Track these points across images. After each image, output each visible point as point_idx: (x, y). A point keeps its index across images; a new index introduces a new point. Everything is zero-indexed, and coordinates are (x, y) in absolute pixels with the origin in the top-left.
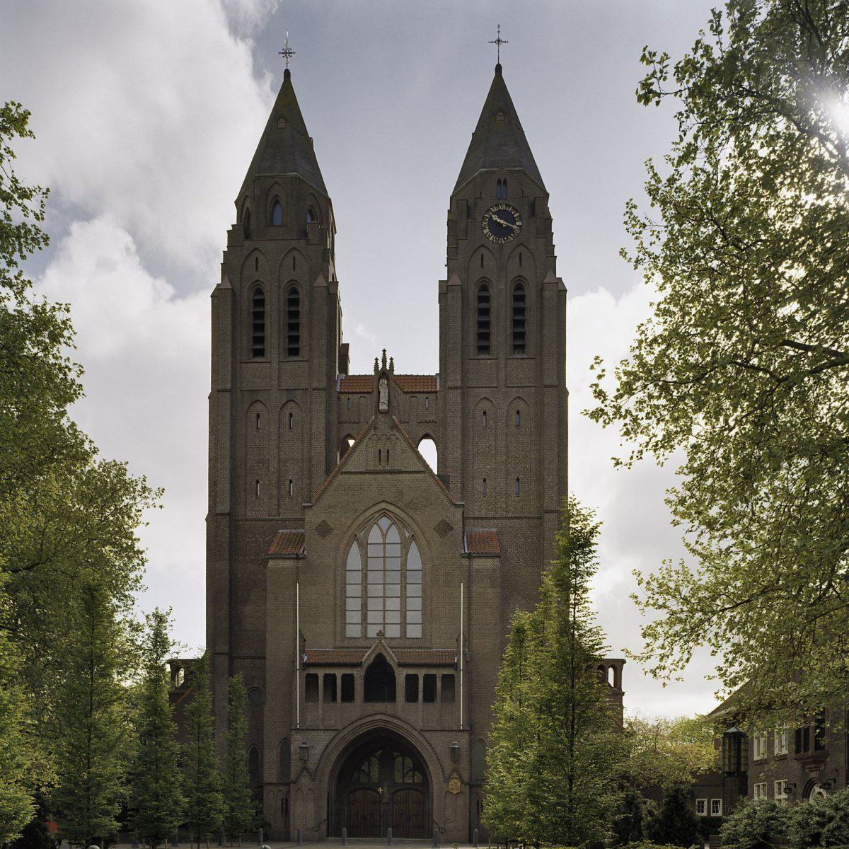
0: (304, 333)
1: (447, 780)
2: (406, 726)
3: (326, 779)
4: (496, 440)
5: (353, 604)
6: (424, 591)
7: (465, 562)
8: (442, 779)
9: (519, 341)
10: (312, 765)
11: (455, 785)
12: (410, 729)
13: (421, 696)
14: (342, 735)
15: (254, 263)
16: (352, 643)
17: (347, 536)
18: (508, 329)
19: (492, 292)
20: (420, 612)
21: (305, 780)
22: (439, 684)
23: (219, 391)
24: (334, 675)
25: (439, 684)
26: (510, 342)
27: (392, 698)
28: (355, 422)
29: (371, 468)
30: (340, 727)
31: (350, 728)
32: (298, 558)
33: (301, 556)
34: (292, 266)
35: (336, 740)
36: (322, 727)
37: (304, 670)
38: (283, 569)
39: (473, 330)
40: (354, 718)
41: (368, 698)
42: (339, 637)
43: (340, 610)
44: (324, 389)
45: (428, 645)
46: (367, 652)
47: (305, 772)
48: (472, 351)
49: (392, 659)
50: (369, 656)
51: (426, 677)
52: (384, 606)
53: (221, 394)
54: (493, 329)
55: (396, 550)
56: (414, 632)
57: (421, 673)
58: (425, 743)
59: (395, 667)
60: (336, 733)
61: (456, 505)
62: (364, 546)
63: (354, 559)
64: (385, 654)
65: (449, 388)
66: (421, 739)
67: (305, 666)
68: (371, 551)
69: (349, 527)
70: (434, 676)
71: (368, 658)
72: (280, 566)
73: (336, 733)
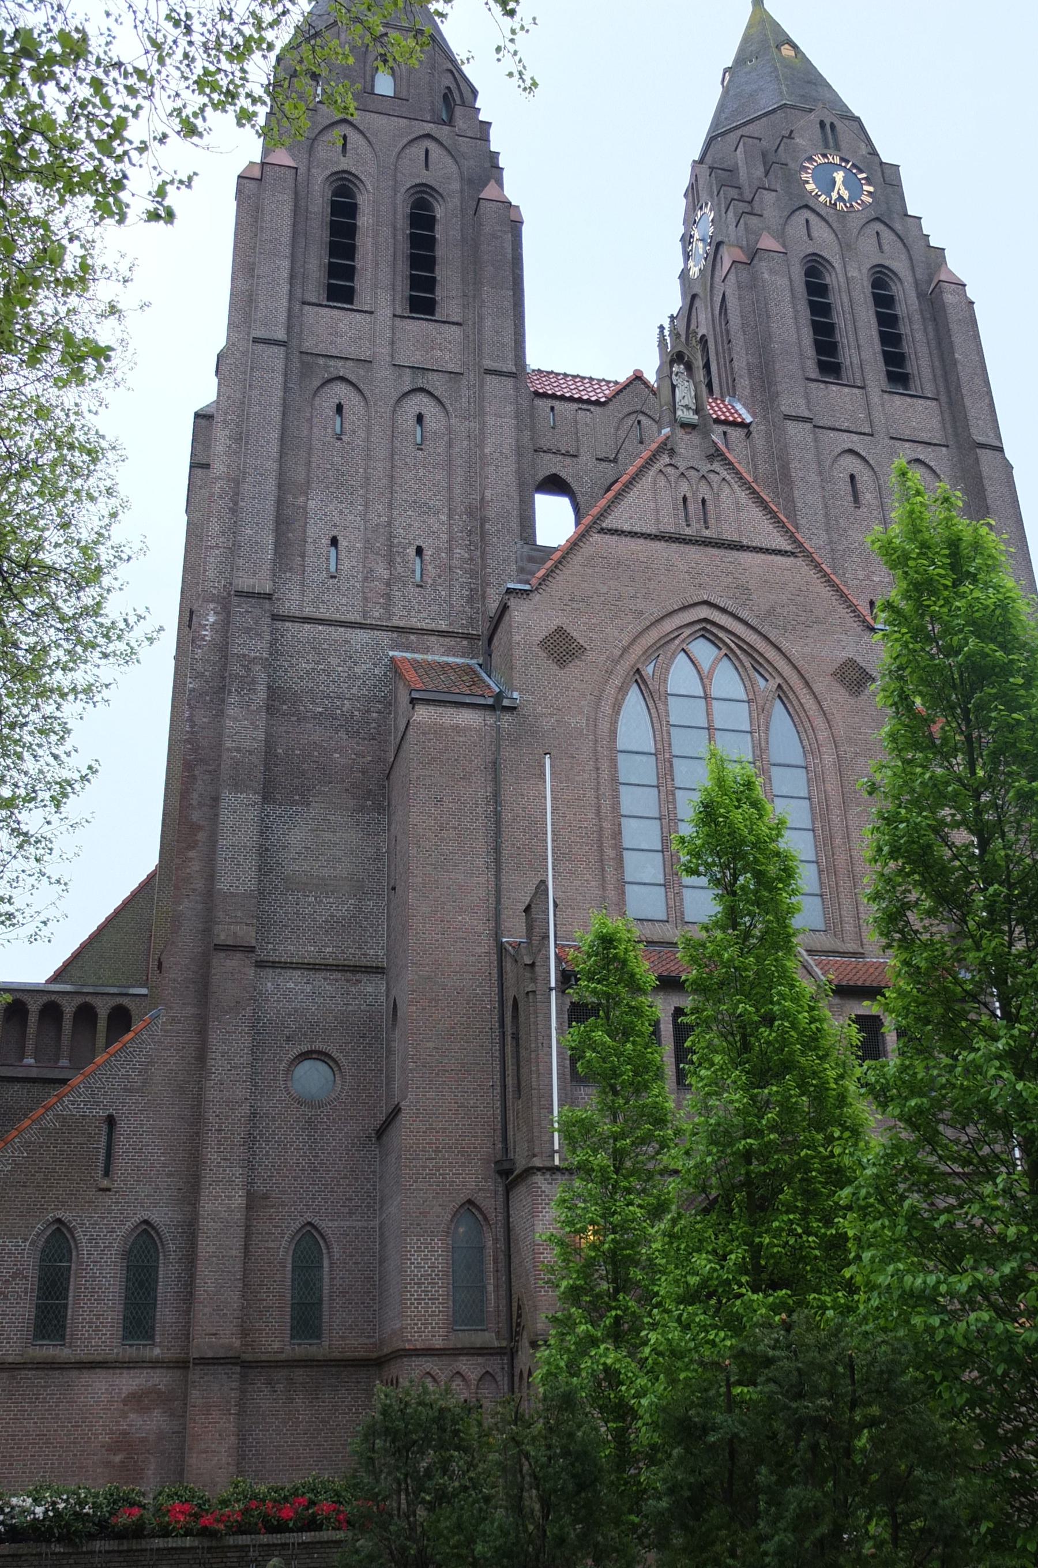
15: (340, 143)
29: (669, 525)
32: (497, 706)
38: (456, 728)
45: (851, 947)
53: (261, 347)
55: (738, 716)
62: (655, 697)
63: (634, 725)
65: (788, 417)
68: (677, 712)
69: (625, 650)
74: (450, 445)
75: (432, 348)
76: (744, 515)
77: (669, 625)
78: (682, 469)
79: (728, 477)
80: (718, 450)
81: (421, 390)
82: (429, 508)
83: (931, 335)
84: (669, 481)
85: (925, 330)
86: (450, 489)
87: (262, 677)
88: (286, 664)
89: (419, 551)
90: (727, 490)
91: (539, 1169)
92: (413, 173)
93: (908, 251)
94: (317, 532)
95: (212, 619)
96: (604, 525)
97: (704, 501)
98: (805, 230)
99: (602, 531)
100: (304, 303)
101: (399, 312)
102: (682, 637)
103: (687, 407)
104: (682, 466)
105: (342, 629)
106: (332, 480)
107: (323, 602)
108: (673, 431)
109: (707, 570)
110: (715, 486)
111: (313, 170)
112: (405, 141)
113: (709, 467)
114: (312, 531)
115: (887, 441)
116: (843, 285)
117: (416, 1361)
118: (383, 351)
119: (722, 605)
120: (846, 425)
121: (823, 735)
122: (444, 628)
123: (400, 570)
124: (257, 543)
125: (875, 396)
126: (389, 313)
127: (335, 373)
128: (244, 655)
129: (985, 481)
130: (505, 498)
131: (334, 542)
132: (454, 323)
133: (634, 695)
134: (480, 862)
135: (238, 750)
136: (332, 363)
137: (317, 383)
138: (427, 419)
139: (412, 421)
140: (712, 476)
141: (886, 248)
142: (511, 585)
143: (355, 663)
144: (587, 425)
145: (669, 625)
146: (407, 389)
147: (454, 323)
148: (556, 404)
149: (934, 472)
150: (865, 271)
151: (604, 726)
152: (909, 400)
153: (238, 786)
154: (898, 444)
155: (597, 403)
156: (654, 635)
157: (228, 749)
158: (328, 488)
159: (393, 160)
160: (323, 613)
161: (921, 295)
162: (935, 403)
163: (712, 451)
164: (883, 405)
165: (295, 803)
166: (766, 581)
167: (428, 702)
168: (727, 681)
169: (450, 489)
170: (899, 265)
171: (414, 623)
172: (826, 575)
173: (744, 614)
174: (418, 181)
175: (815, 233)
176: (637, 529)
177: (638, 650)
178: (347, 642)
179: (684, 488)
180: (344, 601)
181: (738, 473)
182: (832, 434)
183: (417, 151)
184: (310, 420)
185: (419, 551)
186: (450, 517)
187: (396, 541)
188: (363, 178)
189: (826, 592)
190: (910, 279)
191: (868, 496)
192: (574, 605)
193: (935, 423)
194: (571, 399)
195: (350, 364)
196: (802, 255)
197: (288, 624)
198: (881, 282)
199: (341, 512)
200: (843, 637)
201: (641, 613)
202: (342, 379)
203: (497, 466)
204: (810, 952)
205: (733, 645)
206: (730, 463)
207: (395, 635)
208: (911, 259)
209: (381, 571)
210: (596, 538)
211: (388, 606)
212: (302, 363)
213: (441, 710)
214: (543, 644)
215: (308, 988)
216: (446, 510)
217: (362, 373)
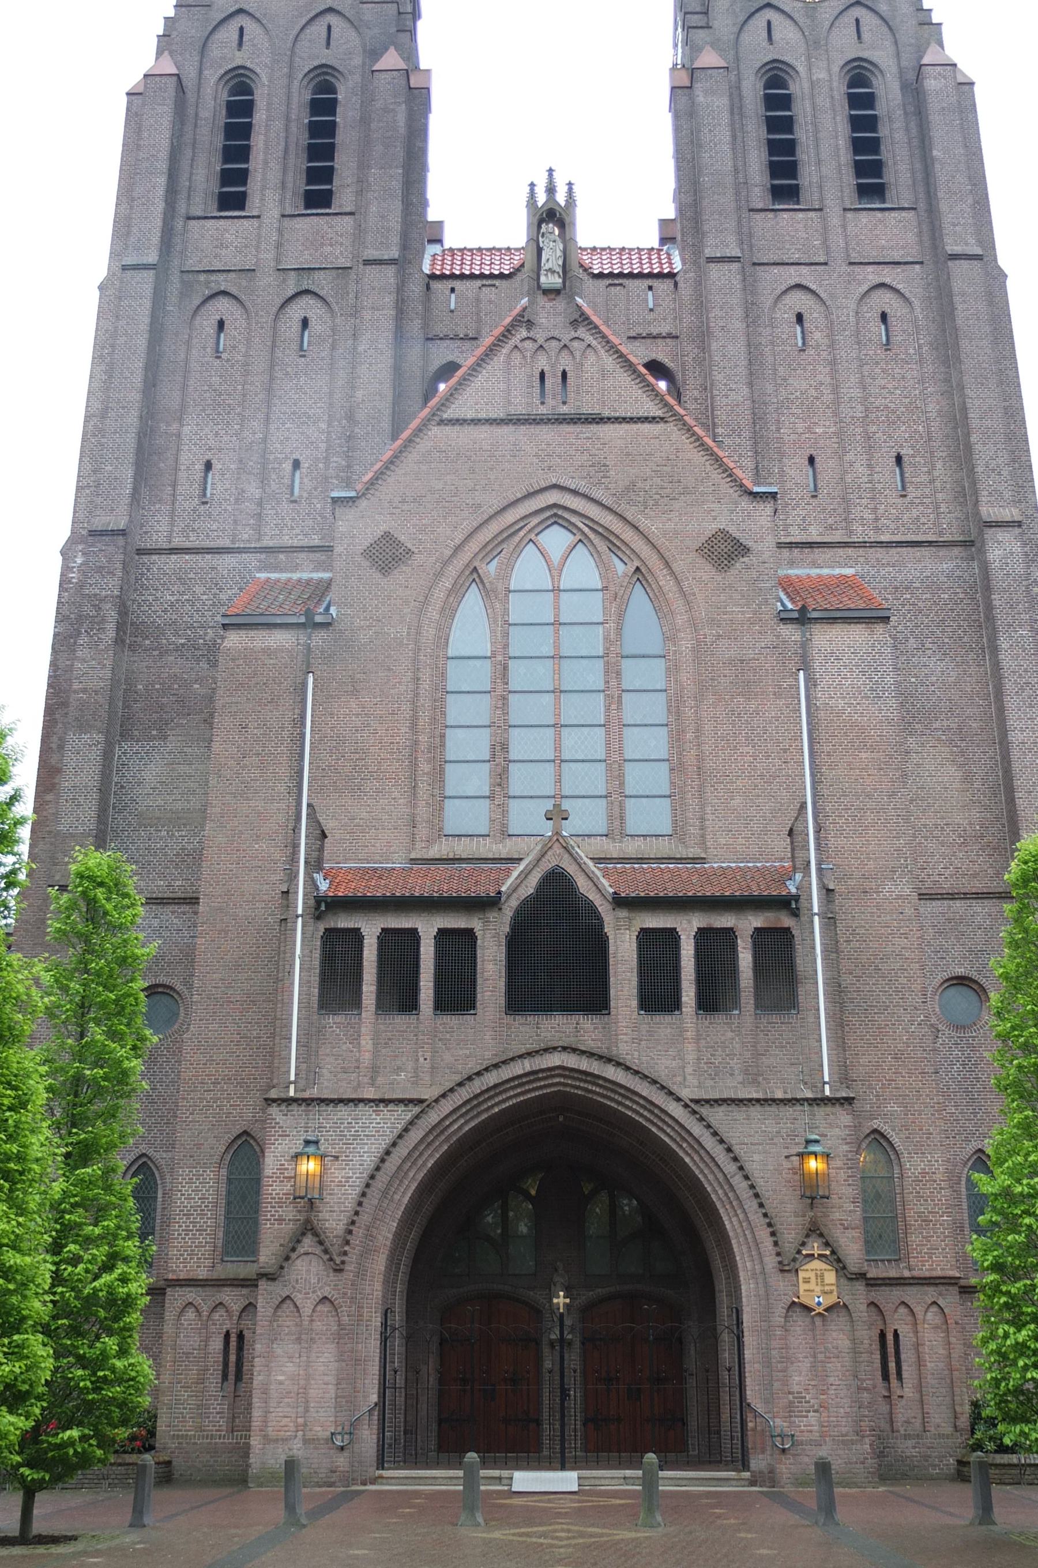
0: (345, 164)
1: (788, 1267)
2: (644, 1089)
3: (379, 1263)
4: (834, 372)
5: (468, 744)
6: (675, 708)
7: (791, 633)
8: (771, 1261)
9: (870, 183)
10: (333, 1220)
11: (817, 1284)
12: (659, 1098)
13: (688, 994)
14: (433, 1117)
15: (235, 36)
16: (462, 848)
17: (452, 571)
18: (842, 152)
19: (797, 88)
20: (665, 767)
21: (308, 1273)
22: (745, 958)
23: (125, 268)
24: (413, 933)
25: (745, 958)
26: (850, 180)
27: (595, 1000)
28: (466, 338)
29: (520, 406)
30: (428, 1094)
31: (464, 1094)
32: (310, 625)
33: (318, 619)
34: (324, 43)
35: (415, 1135)
36: (370, 1093)
37: (318, 917)
38: (267, 651)
39: (757, 160)
40: (473, 1066)
41: (521, 999)
42: (422, 831)
43: (426, 761)
44: (392, 262)
45: (693, 852)
46: (509, 871)
47: (308, 1243)
48: (759, 196)
49: (596, 887)
50: (526, 874)
51: (703, 935)
52: (558, 748)
53: (129, 273)
54: (805, 155)
55: (593, 607)
56: (650, 818)
57: (687, 927)
58: (709, 1142)
59: (604, 908)
60: (417, 1110)
61: (751, 493)
62: (496, 596)
63: (470, 629)
64: (571, 869)
65: (711, 260)
66: (697, 1129)
67: (324, 906)
68: (518, 609)
69: (458, 549)
70: (729, 933)
71: (519, 885)
72: (258, 644)
73: (417, 1110)
74: (333, 348)
75: (322, 245)
76: (609, 383)
77: (511, 517)
78: (541, 341)
79: (594, 343)
80: (583, 314)
81: (307, 292)
82: (309, 417)
83: (914, 132)
84: (524, 357)
85: (907, 130)
86: (331, 394)
87: (111, 614)
88: (150, 598)
89: (296, 464)
90: (592, 358)
91: (274, 1101)
92: (313, 52)
93: (894, 35)
94: (190, 459)
95: (79, 560)
96: (445, 416)
97: (564, 374)
98: (765, 34)
99: (442, 422)
100: (189, 218)
101: (289, 211)
102: (529, 527)
103: (552, 271)
104: (541, 337)
105: (209, 556)
106: (210, 402)
107: (193, 530)
108: (531, 302)
109: (558, 450)
110: (578, 354)
111: (206, 72)
112: (304, 21)
113: (573, 334)
114: (185, 458)
115: (845, 268)
116: (806, 91)
117: (179, 1291)
118: (268, 256)
119: (573, 487)
120: (796, 257)
121: (681, 619)
122: (316, 542)
123: (274, 486)
124: (116, 478)
125: (835, 218)
126: (276, 213)
127: (215, 288)
128: (95, 595)
129: (957, 299)
130: (377, 397)
131: (208, 466)
132: (346, 214)
133: (473, 598)
134: (281, 788)
135: (84, 691)
136: (213, 277)
137: (197, 302)
138: (312, 323)
139: (297, 326)
140: (576, 344)
141: (865, 36)
142: (335, 494)
143: (221, 589)
144: (490, 302)
145: (511, 517)
146: (290, 293)
147: (346, 214)
148: (457, 284)
149: (902, 295)
150: (836, 69)
151: (429, 633)
152: (879, 215)
153: (82, 727)
154: (857, 269)
155: (502, 276)
156: (494, 528)
157: (76, 692)
158: (204, 410)
159: (289, 45)
160: (194, 541)
161: (904, 86)
162: (913, 212)
163: (576, 316)
164: (844, 227)
165: (153, 738)
166: (628, 454)
167: (239, 626)
168: (583, 570)
169: (331, 394)
170: (882, 55)
171: (287, 541)
172: (699, 438)
173: (597, 494)
174: (316, 63)
175: (776, 35)
176: (483, 415)
177: (474, 546)
178: (213, 568)
179: (542, 362)
180: (214, 527)
181: (604, 337)
182: (776, 270)
183: (318, 29)
184: (188, 343)
185: (296, 464)
186: (329, 425)
187: (272, 457)
188: (258, 70)
189: (699, 458)
190: (894, 69)
191: (817, 335)
192: (405, 507)
193: (911, 237)
194: (472, 276)
195: (233, 275)
196: (759, 64)
197: (155, 557)
198: (859, 80)
199: (217, 434)
200: (716, 505)
201: (480, 506)
202: (225, 293)
203: (370, 364)
204: (597, 860)
205: (586, 530)
206: (596, 327)
207: (263, 556)
208: (896, 43)
209: (253, 490)
210: (435, 431)
211: (258, 529)
212: (182, 282)
213: (252, 633)
214: (367, 553)
215: (156, 923)
216: (326, 418)
217: (244, 283)
